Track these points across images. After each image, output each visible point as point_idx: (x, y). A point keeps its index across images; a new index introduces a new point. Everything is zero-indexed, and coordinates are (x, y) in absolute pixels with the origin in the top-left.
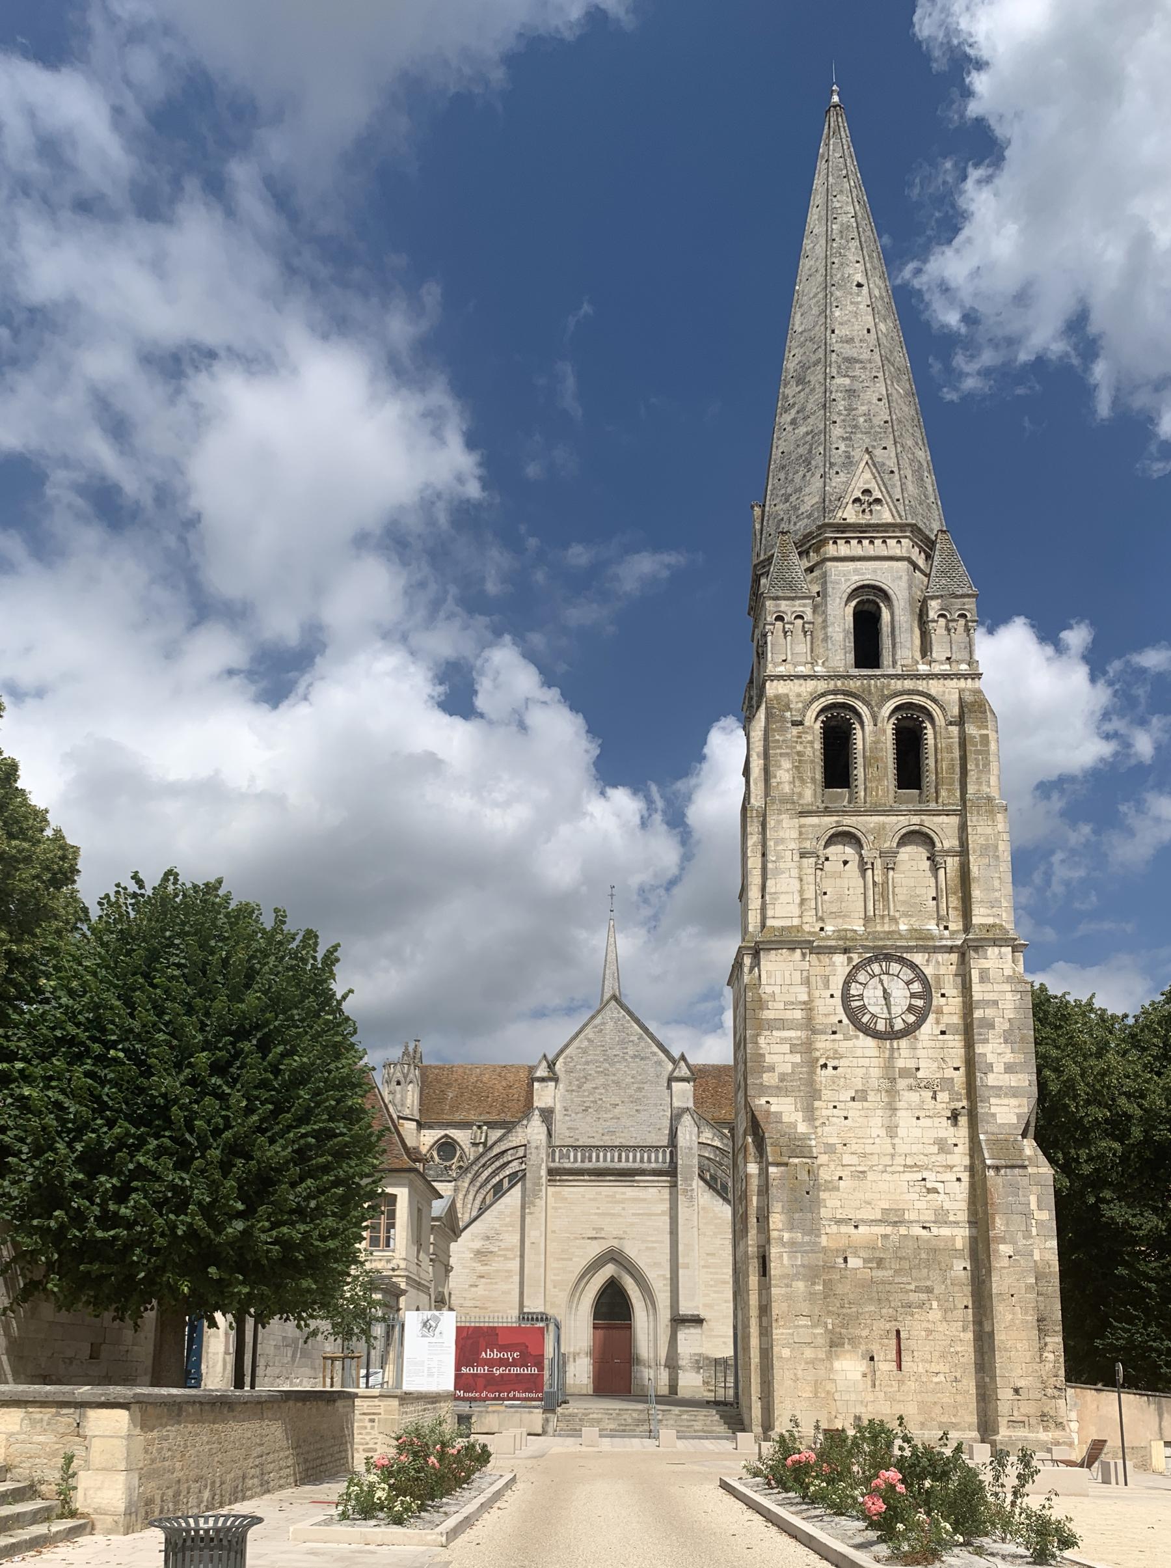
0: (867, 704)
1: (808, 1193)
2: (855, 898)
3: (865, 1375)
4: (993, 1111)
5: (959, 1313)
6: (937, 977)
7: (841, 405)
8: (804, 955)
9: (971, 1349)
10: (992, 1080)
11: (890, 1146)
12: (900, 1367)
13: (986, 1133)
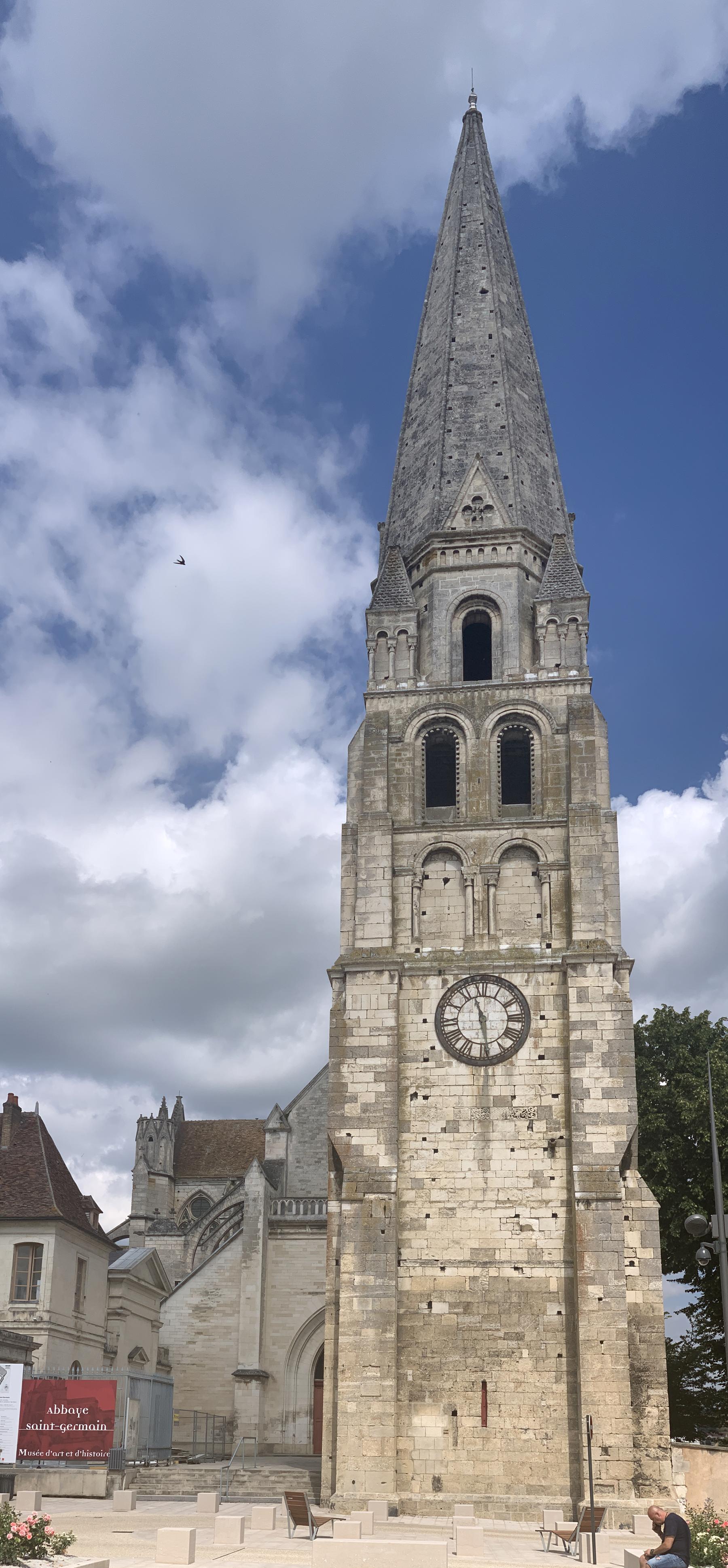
0: (470, 716)
1: (383, 1232)
2: (455, 917)
3: (446, 1432)
4: (588, 1140)
5: (552, 1362)
6: (537, 998)
7: (457, 414)
8: (392, 977)
9: (564, 1403)
10: (588, 1106)
11: (481, 1181)
12: (484, 1423)
13: (581, 1164)
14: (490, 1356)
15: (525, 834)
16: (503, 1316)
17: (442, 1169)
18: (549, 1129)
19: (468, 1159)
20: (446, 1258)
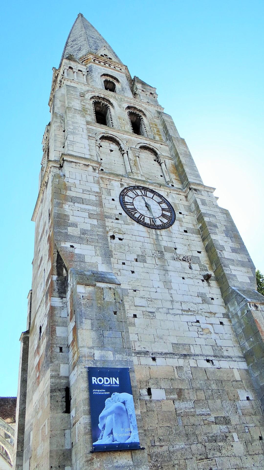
14: (210, 441)
16: (209, 401)
17: (140, 284)
18: (202, 270)
20: (155, 350)
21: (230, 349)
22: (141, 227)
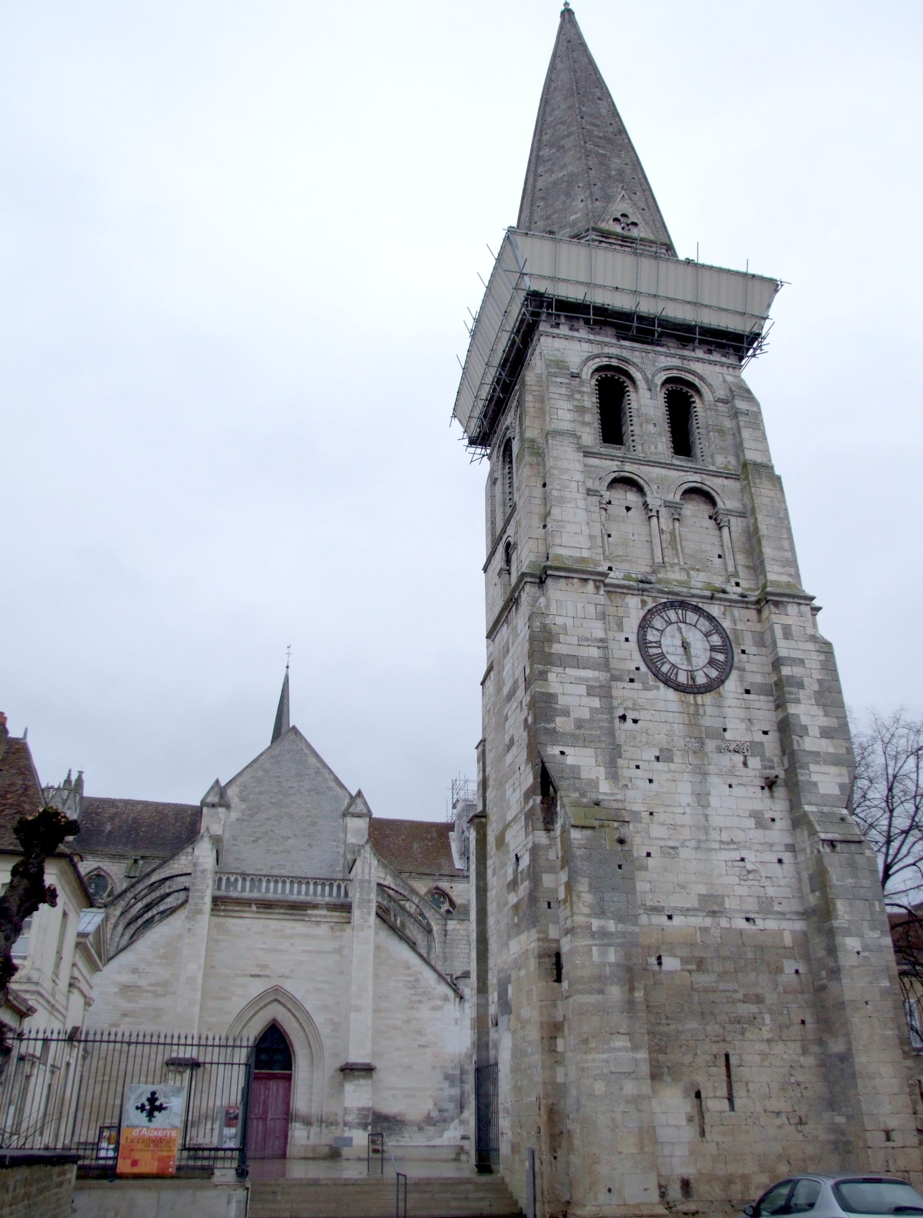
3: (690, 1119)
11: (702, 818)
14: (731, 1022)
15: (702, 479)
16: (739, 974)
18: (765, 767)
19: (684, 792)
20: (673, 904)
21: (784, 901)
22: (671, 694)
